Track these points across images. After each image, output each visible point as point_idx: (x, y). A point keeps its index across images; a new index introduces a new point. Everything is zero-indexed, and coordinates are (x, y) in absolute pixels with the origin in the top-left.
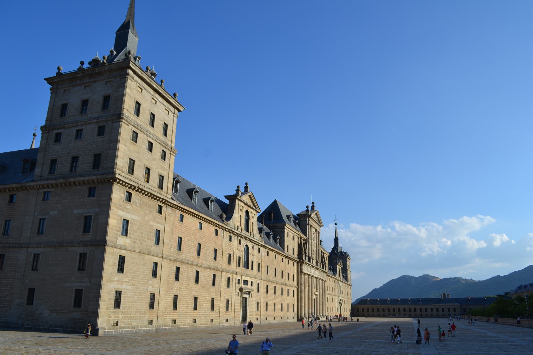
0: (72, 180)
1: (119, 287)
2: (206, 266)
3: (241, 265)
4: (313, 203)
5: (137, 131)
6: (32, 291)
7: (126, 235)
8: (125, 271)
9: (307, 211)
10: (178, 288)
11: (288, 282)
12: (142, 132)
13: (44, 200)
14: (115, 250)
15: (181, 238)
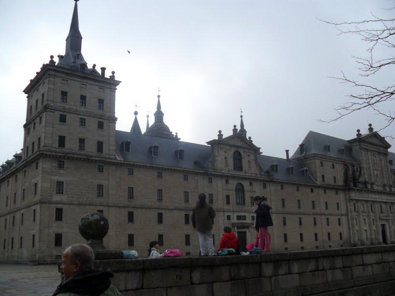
0: (28, 160)
1: (59, 231)
2: (173, 208)
3: (231, 201)
4: (370, 125)
5: (65, 114)
6: (21, 237)
7: (62, 193)
8: (63, 219)
9: (359, 135)
10: (131, 229)
11: (326, 212)
12: (70, 113)
13: (25, 175)
14: (51, 205)
15: (133, 188)
